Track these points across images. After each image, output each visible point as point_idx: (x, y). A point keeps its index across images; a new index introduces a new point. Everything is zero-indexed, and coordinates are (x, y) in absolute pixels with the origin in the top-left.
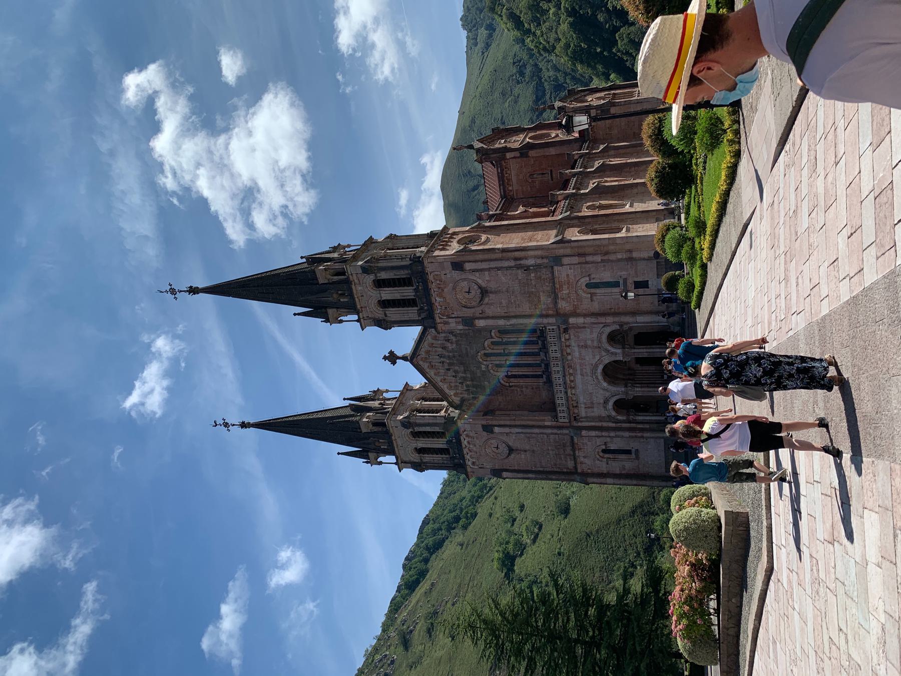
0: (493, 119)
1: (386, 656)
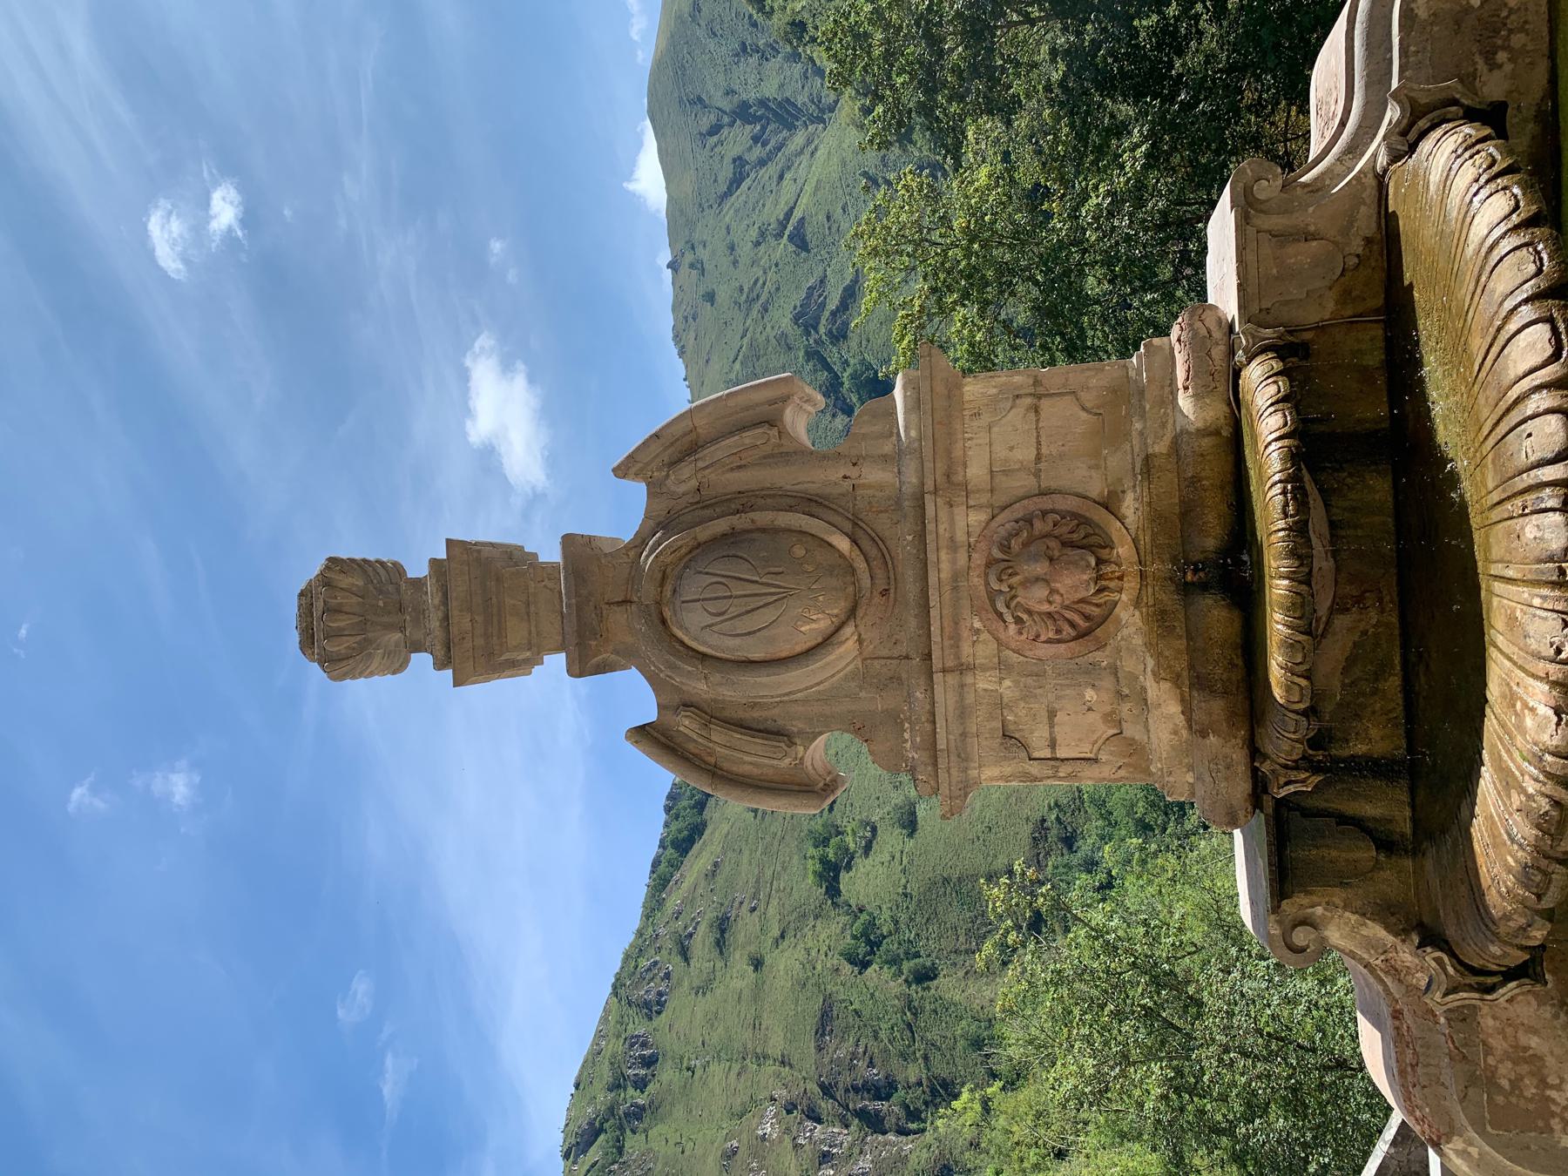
0: (734, 11)
1: (656, 963)
